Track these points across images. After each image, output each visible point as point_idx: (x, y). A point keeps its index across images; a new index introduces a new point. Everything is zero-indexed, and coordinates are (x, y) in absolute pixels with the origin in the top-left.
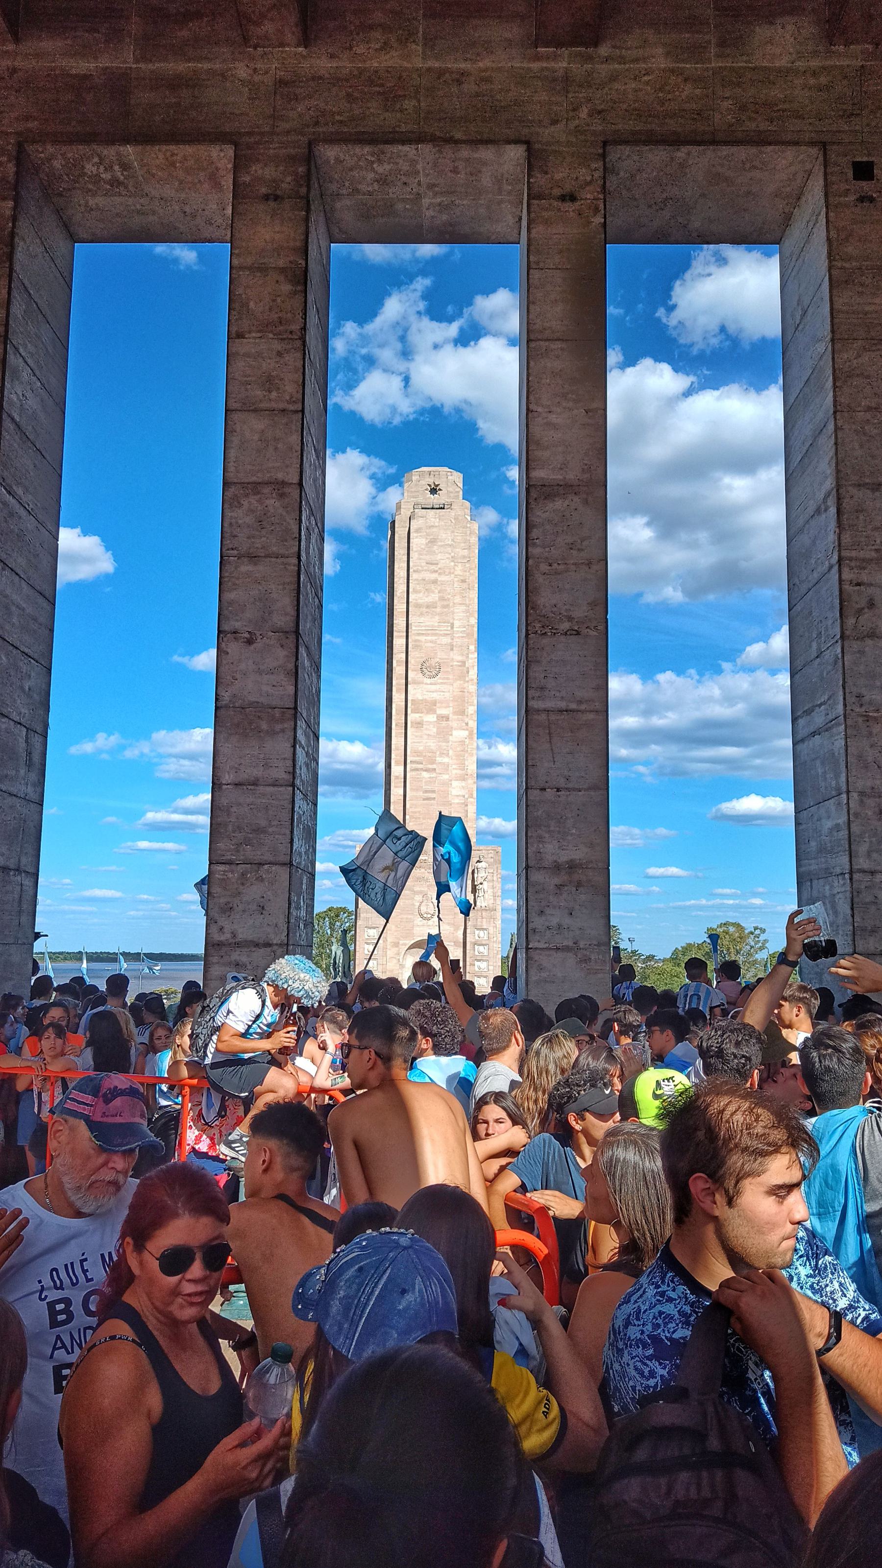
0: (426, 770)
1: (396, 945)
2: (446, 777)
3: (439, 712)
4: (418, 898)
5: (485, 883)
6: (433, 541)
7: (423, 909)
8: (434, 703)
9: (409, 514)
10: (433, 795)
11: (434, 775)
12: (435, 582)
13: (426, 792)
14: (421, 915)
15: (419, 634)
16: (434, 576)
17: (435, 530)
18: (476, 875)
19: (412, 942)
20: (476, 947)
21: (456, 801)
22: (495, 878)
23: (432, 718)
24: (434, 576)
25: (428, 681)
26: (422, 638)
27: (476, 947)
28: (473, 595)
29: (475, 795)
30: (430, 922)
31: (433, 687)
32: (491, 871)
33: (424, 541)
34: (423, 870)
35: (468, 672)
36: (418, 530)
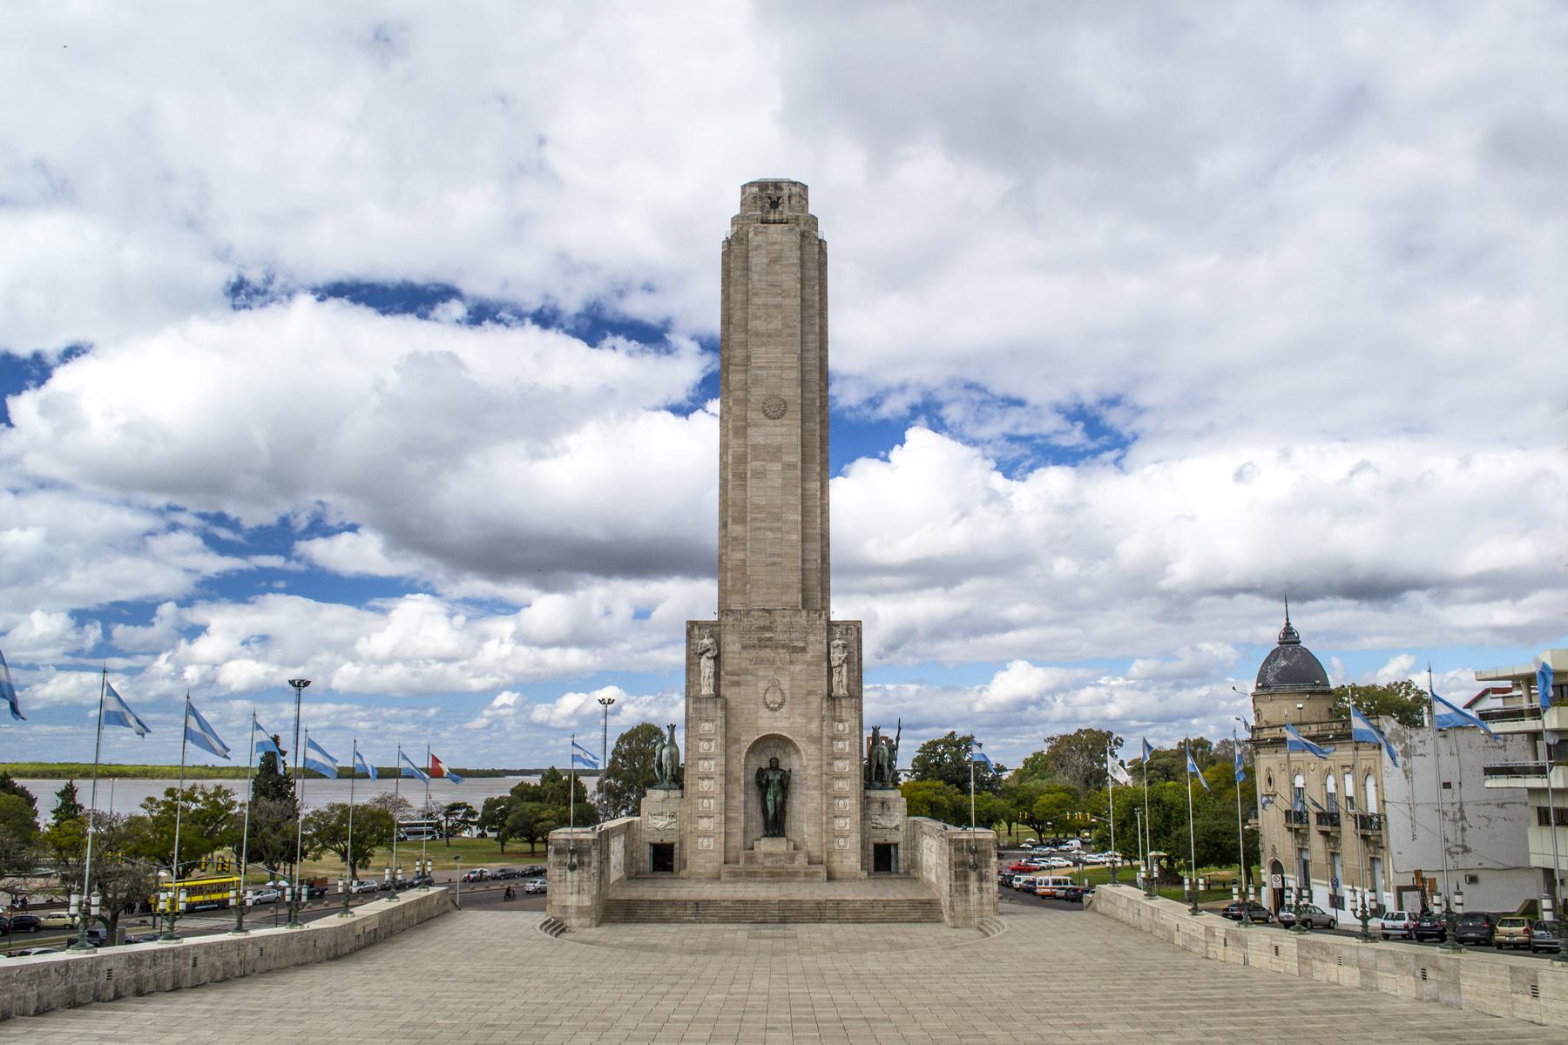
3: (786, 459)
4: (763, 684)
6: (775, 261)
7: (769, 698)
8: (779, 448)
12: (778, 306)
13: (772, 555)
14: (767, 706)
15: (759, 368)
23: (777, 467)
24: (779, 299)
25: (771, 422)
26: (764, 373)
31: (778, 430)
33: (765, 260)
36: (758, 247)
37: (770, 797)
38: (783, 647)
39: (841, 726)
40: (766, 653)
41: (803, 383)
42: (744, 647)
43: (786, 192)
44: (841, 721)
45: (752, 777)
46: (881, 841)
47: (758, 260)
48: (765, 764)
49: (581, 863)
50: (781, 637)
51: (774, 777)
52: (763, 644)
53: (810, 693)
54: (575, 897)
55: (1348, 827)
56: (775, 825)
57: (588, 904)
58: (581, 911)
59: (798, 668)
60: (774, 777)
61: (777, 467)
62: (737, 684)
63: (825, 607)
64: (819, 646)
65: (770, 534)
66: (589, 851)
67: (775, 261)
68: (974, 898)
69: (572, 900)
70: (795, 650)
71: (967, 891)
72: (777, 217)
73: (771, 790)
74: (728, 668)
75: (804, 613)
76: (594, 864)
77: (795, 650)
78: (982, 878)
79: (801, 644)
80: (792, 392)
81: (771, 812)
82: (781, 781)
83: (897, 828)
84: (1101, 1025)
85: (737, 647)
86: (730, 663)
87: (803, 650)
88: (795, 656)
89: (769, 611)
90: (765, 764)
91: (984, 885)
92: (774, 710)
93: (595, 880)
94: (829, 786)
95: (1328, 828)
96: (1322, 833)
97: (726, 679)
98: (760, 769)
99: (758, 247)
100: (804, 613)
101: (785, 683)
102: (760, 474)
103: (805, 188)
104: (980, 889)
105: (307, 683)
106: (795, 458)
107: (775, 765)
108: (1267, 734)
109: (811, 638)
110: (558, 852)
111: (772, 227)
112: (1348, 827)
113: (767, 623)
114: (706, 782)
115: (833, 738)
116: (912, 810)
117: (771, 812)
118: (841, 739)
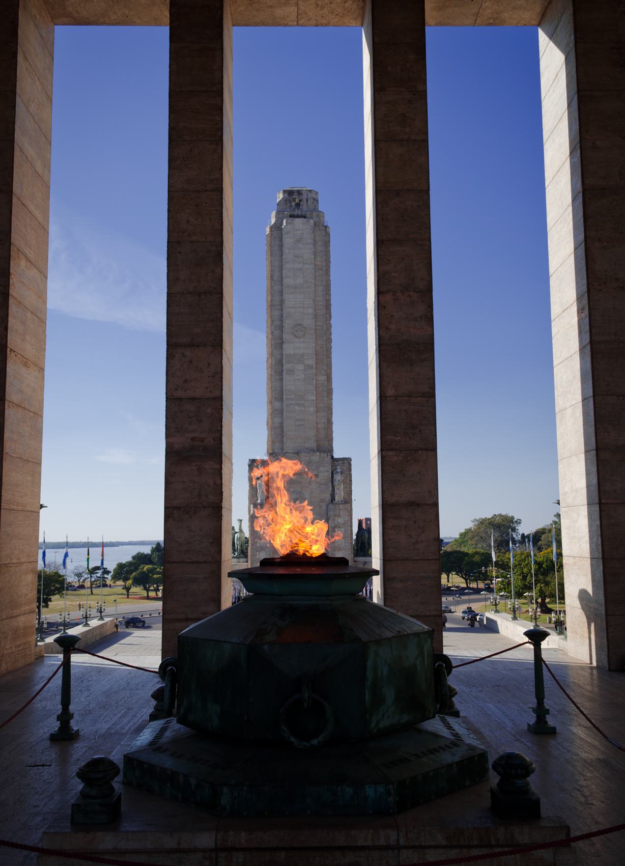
3: (306, 362)
6: (299, 240)
12: (301, 269)
16: (300, 266)
23: (301, 367)
24: (300, 266)
25: (297, 340)
39: (340, 520)
41: (316, 316)
43: (304, 197)
47: (288, 241)
61: (301, 367)
63: (331, 451)
64: (326, 474)
65: (297, 408)
75: (318, 454)
80: (308, 322)
99: (288, 233)
102: (291, 372)
103: (317, 193)
106: (311, 362)
109: (322, 469)
111: (297, 220)
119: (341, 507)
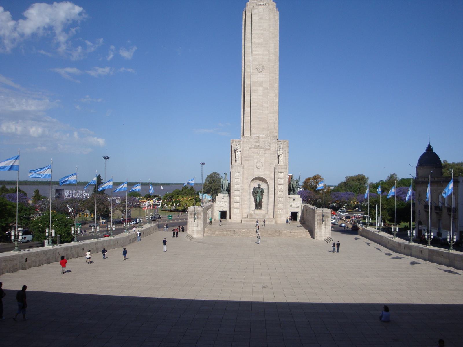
0: (259, 109)
1: (247, 179)
2: (267, 112)
3: (264, 86)
4: (256, 161)
5: (283, 155)
6: (261, 18)
7: (258, 165)
9: (251, 7)
10: (261, 120)
11: (262, 111)
12: (262, 34)
14: (257, 167)
17: (262, 13)
18: (279, 151)
19: (253, 178)
20: (279, 180)
21: (271, 122)
22: (286, 153)
23: (261, 88)
25: (259, 73)
26: (257, 57)
27: (279, 180)
28: (277, 39)
29: (278, 120)
30: (260, 170)
32: (285, 150)
34: (258, 149)
35: (275, 70)
37: (258, 197)
38: (263, 148)
40: (256, 150)
42: (250, 148)
44: (281, 173)
45: (252, 191)
46: (293, 211)
48: (256, 186)
49: (198, 218)
50: (262, 145)
51: (259, 191)
52: (256, 147)
53: (271, 163)
54: (196, 228)
55: (445, 211)
56: (259, 205)
57: (201, 230)
58: (198, 232)
59: (267, 155)
60: (259, 191)
62: (247, 160)
64: (274, 148)
65: (258, 111)
66: (200, 214)
67: (261, 18)
68: (323, 230)
69: (195, 229)
70: (266, 149)
71: (321, 228)
72: (262, 3)
73: (258, 195)
74: (244, 155)
76: (202, 218)
77: (266, 149)
78: (325, 225)
79: (268, 148)
81: (258, 201)
82: (261, 192)
83: (298, 207)
84: (367, 277)
85: (247, 148)
86: (245, 153)
87: (269, 149)
88: (266, 152)
89: (258, 137)
90: (256, 186)
91: (326, 227)
92: (260, 169)
93: (202, 222)
94: (277, 193)
95: (438, 211)
96: (436, 213)
97: (244, 158)
98: (255, 188)
100: (269, 137)
101: (263, 160)
104: (325, 228)
105: (108, 158)
107: (259, 187)
108: (420, 180)
109: (272, 146)
110: (191, 214)
112: (445, 211)
113: (258, 140)
114: (237, 192)
115: (278, 178)
116: (303, 201)
117: (258, 201)
118: (281, 179)
119: (282, 167)
